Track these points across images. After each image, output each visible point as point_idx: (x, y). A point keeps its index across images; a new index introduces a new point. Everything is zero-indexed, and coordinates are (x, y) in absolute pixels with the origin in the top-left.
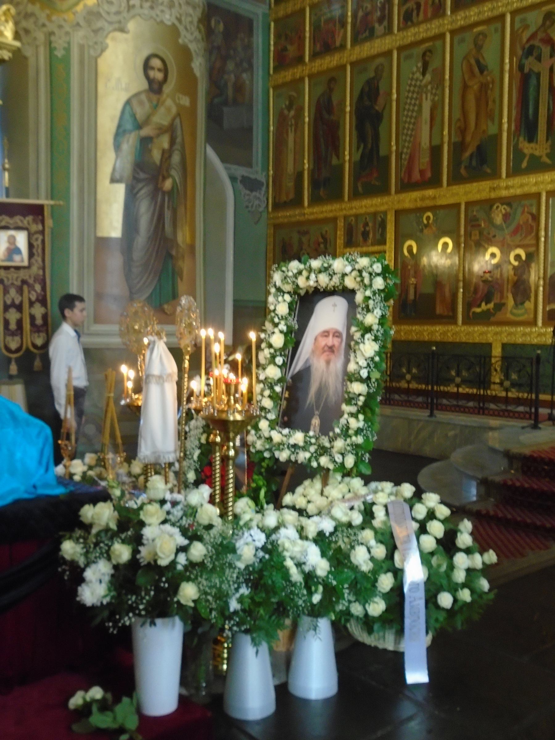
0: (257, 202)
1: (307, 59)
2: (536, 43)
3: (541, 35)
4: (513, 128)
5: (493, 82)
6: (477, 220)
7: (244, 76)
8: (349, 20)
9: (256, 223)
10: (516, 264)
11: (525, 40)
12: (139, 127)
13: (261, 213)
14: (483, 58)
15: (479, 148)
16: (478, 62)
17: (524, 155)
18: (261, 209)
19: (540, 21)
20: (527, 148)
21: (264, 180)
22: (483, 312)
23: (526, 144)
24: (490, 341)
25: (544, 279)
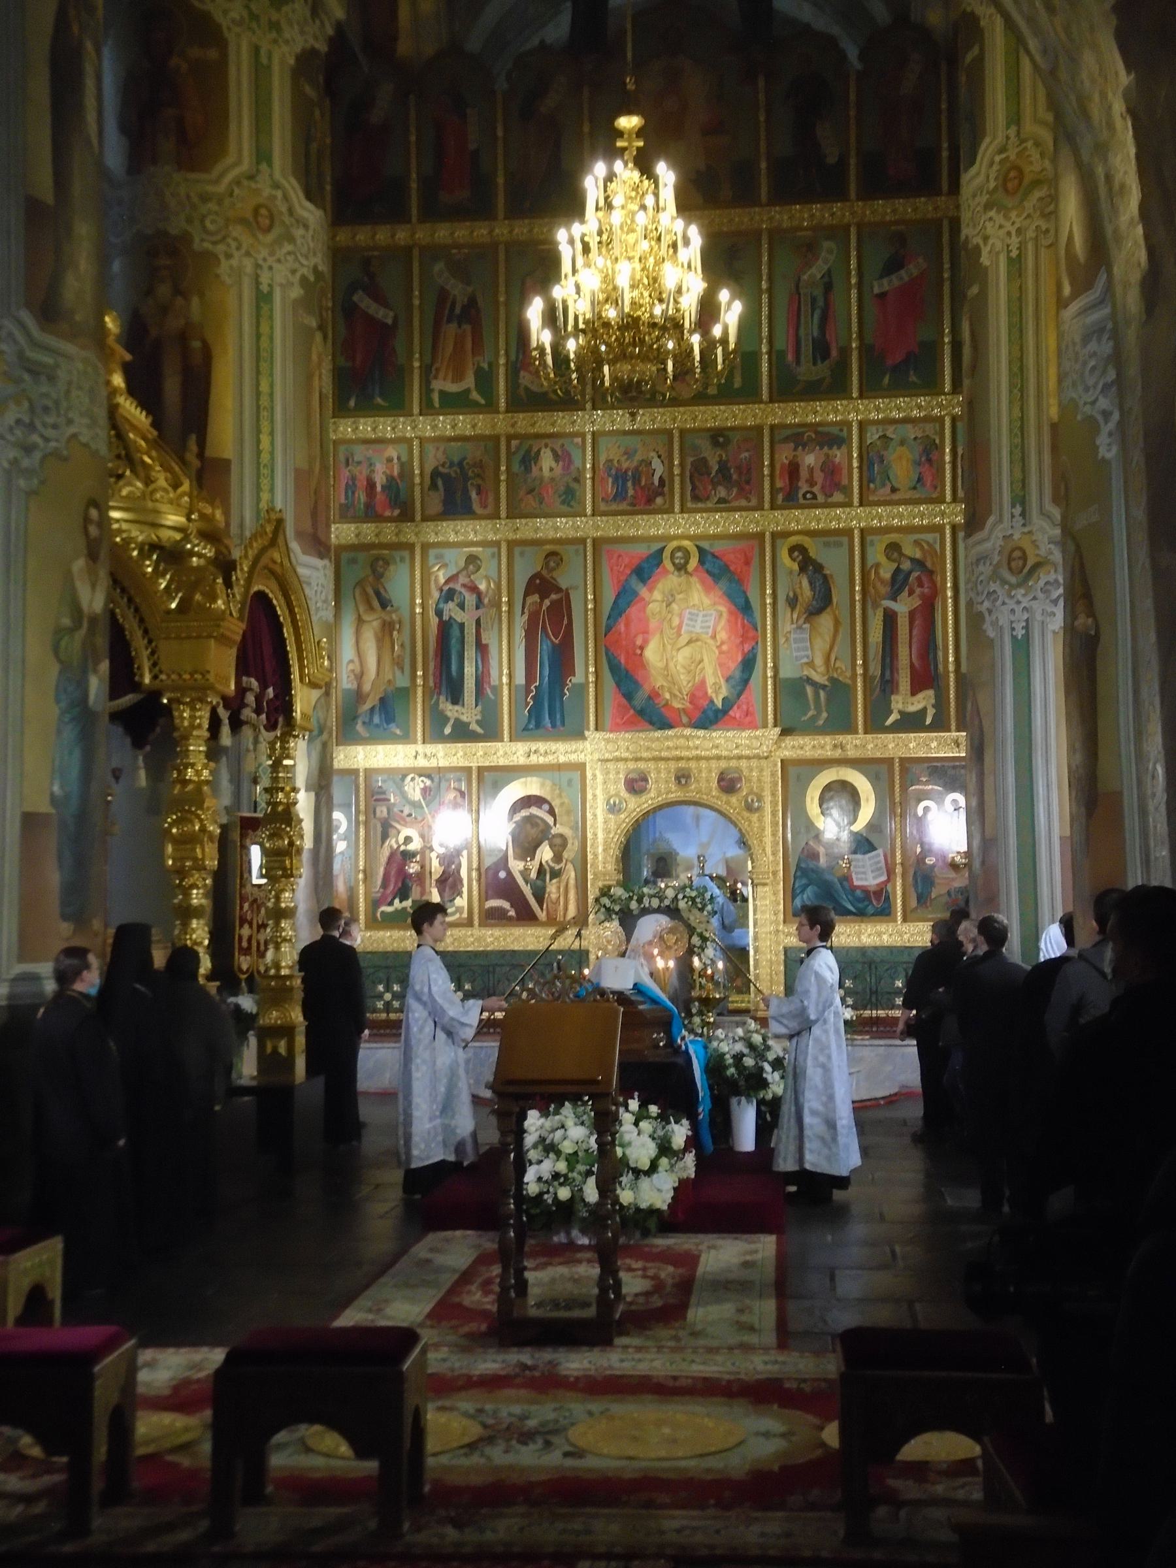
2: (458, 587)
3: (462, 579)
4: (431, 684)
5: (400, 622)
6: (384, 793)
10: (442, 851)
11: (442, 580)
12: (321, 732)
14: (386, 590)
15: (382, 700)
16: (378, 594)
17: (447, 719)
19: (462, 564)
20: (451, 710)
22: (396, 910)
23: (449, 706)
24: (409, 949)
25: (479, 869)
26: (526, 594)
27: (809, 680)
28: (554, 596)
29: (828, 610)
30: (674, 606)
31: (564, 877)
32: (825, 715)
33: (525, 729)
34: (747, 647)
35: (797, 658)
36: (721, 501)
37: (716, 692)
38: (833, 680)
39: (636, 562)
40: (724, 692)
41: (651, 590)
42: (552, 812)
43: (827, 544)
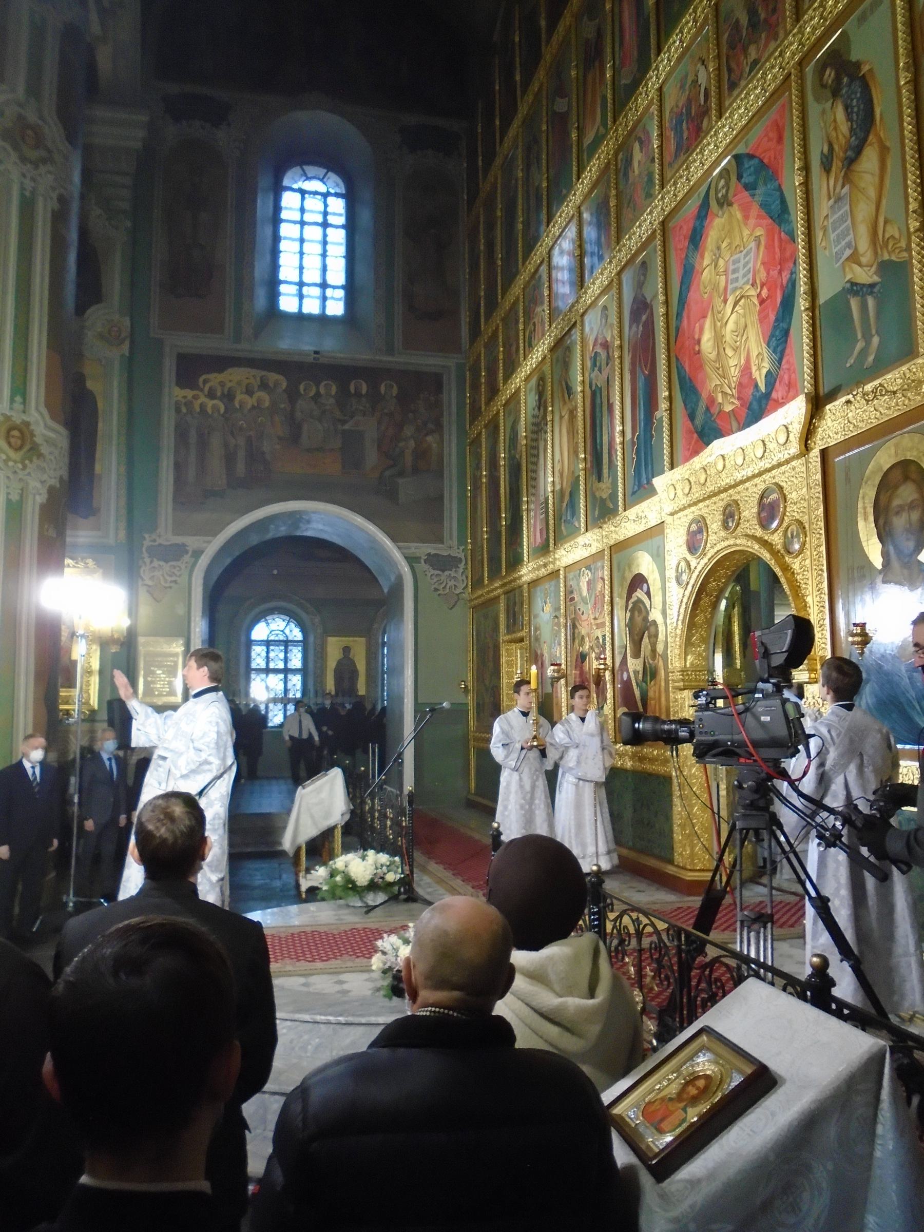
0: (451, 583)
1: (483, 409)
5: (576, 408)
7: (429, 439)
8: (501, 357)
9: (454, 606)
13: (458, 595)
18: (457, 592)
21: (462, 556)
26: (630, 327)
27: (855, 288)
28: (644, 318)
29: (871, 138)
30: (721, 262)
31: (658, 678)
32: (876, 340)
33: (634, 493)
34: (786, 276)
35: (838, 256)
36: (755, 63)
37: (759, 369)
38: (884, 267)
39: (691, 225)
40: (766, 366)
41: (702, 257)
42: (648, 594)
43: (863, 19)
